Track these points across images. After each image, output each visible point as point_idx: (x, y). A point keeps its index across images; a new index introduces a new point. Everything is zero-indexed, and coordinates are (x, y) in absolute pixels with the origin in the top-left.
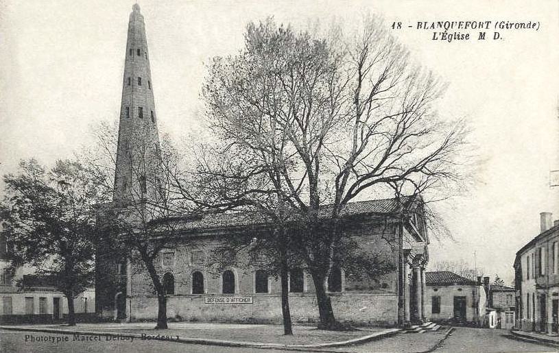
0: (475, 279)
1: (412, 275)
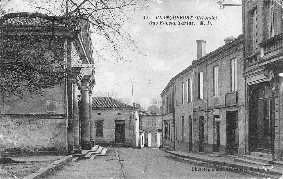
0: (131, 105)
1: (81, 97)
